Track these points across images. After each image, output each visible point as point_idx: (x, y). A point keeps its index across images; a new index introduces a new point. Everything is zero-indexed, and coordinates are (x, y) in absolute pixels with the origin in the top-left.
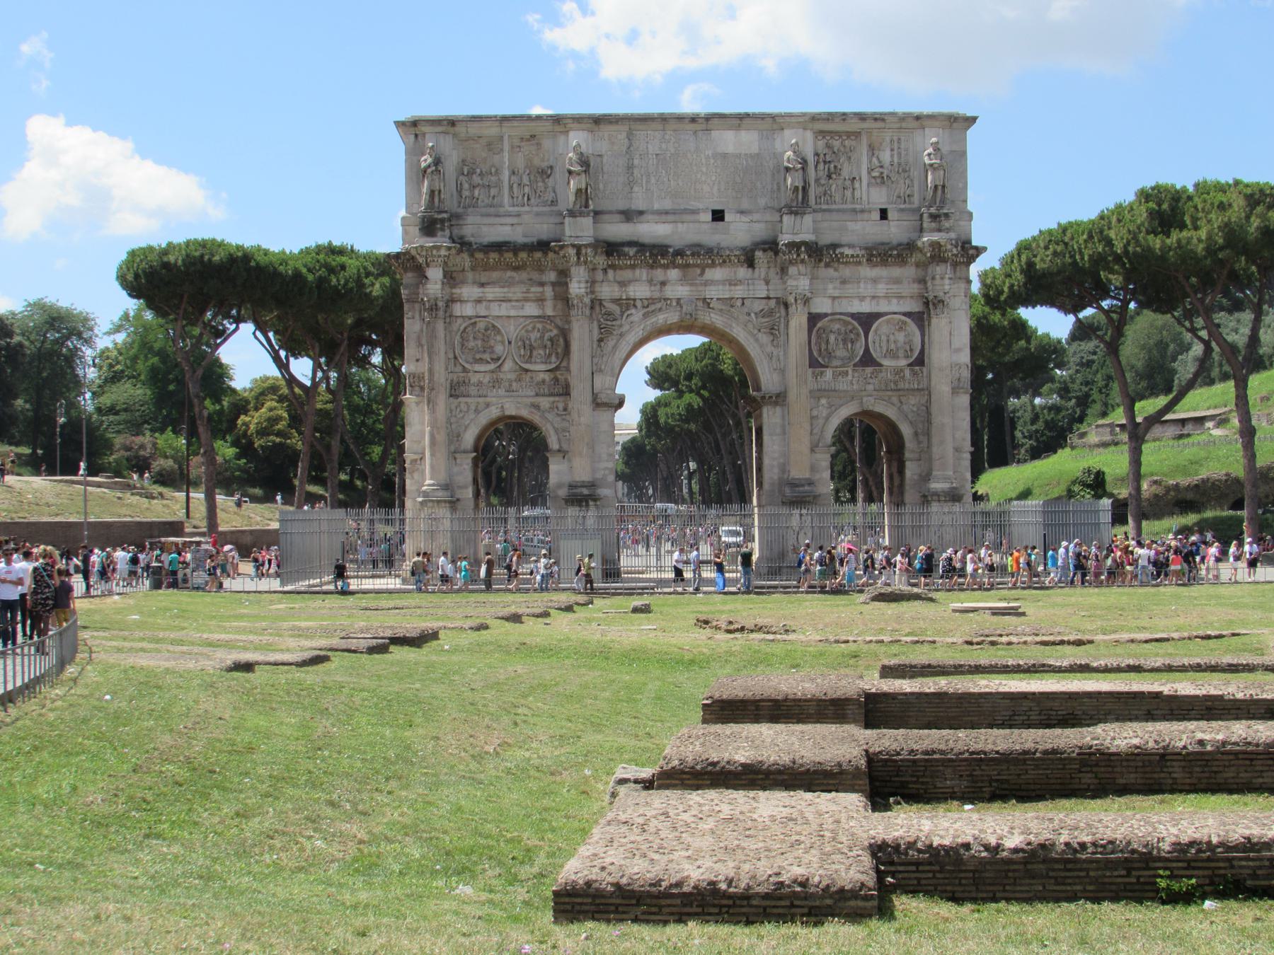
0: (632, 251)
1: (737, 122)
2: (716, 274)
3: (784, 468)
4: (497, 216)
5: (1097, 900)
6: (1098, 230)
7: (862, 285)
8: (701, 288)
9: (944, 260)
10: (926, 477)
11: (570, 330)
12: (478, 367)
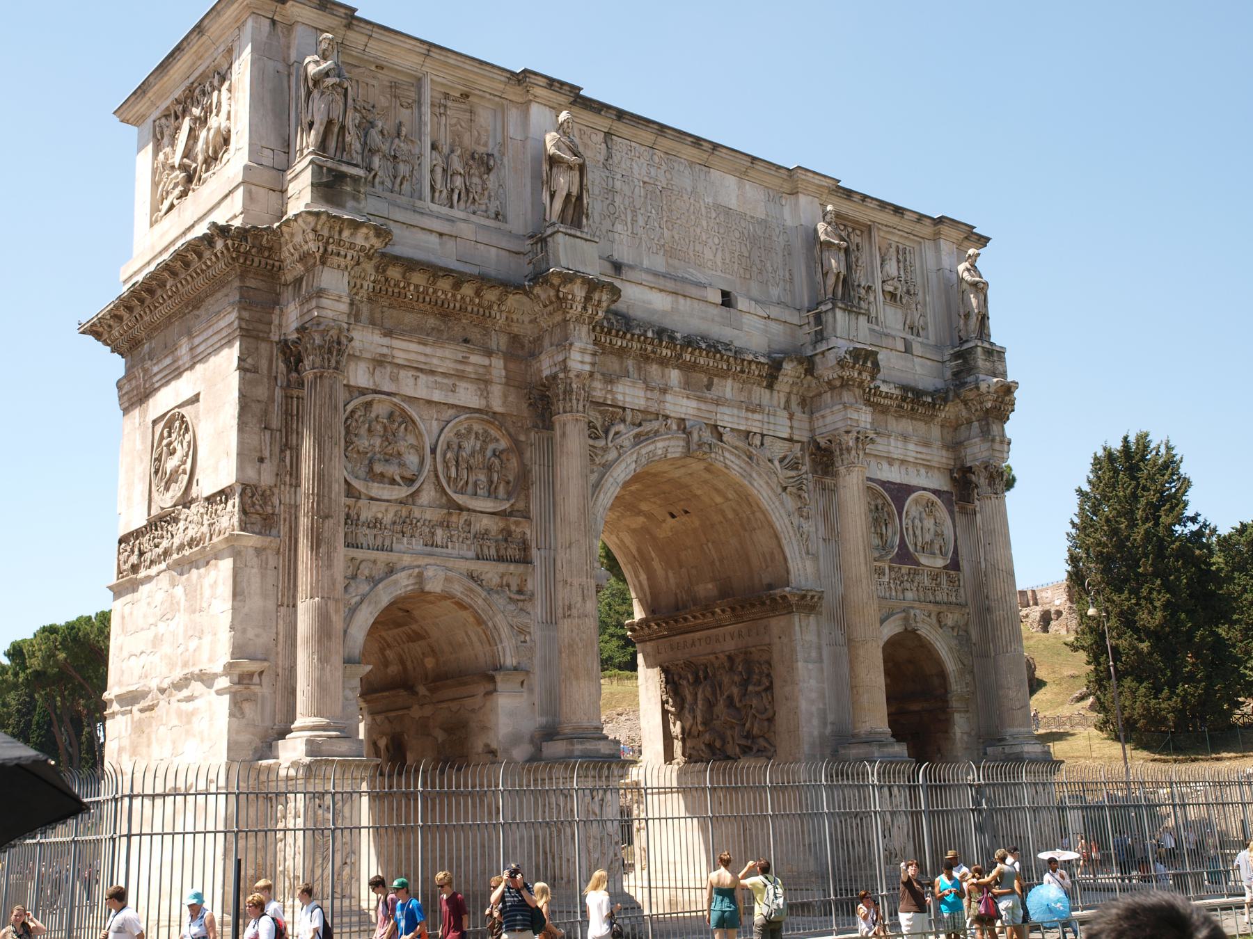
2: (727, 388)
4: (415, 210)
8: (712, 408)
12: (377, 490)
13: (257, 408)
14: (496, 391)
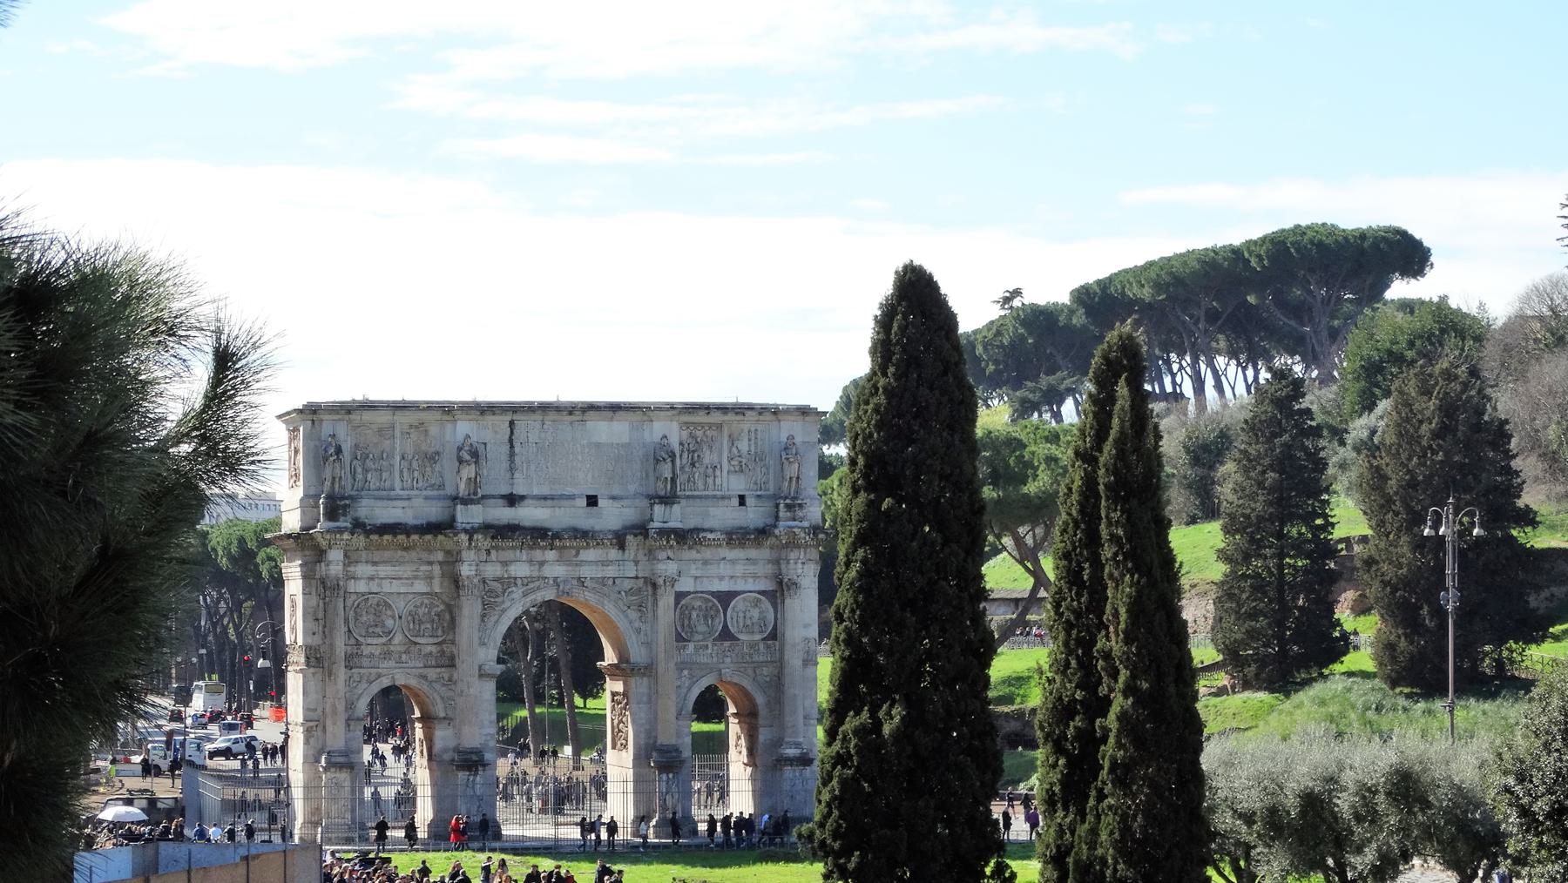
1: (610, 414)
2: (590, 554)
4: (390, 499)
7: (722, 566)
8: (577, 568)
9: (798, 547)
10: (778, 743)
11: (460, 607)
12: (370, 640)
13: (311, 610)
14: (436, 582)
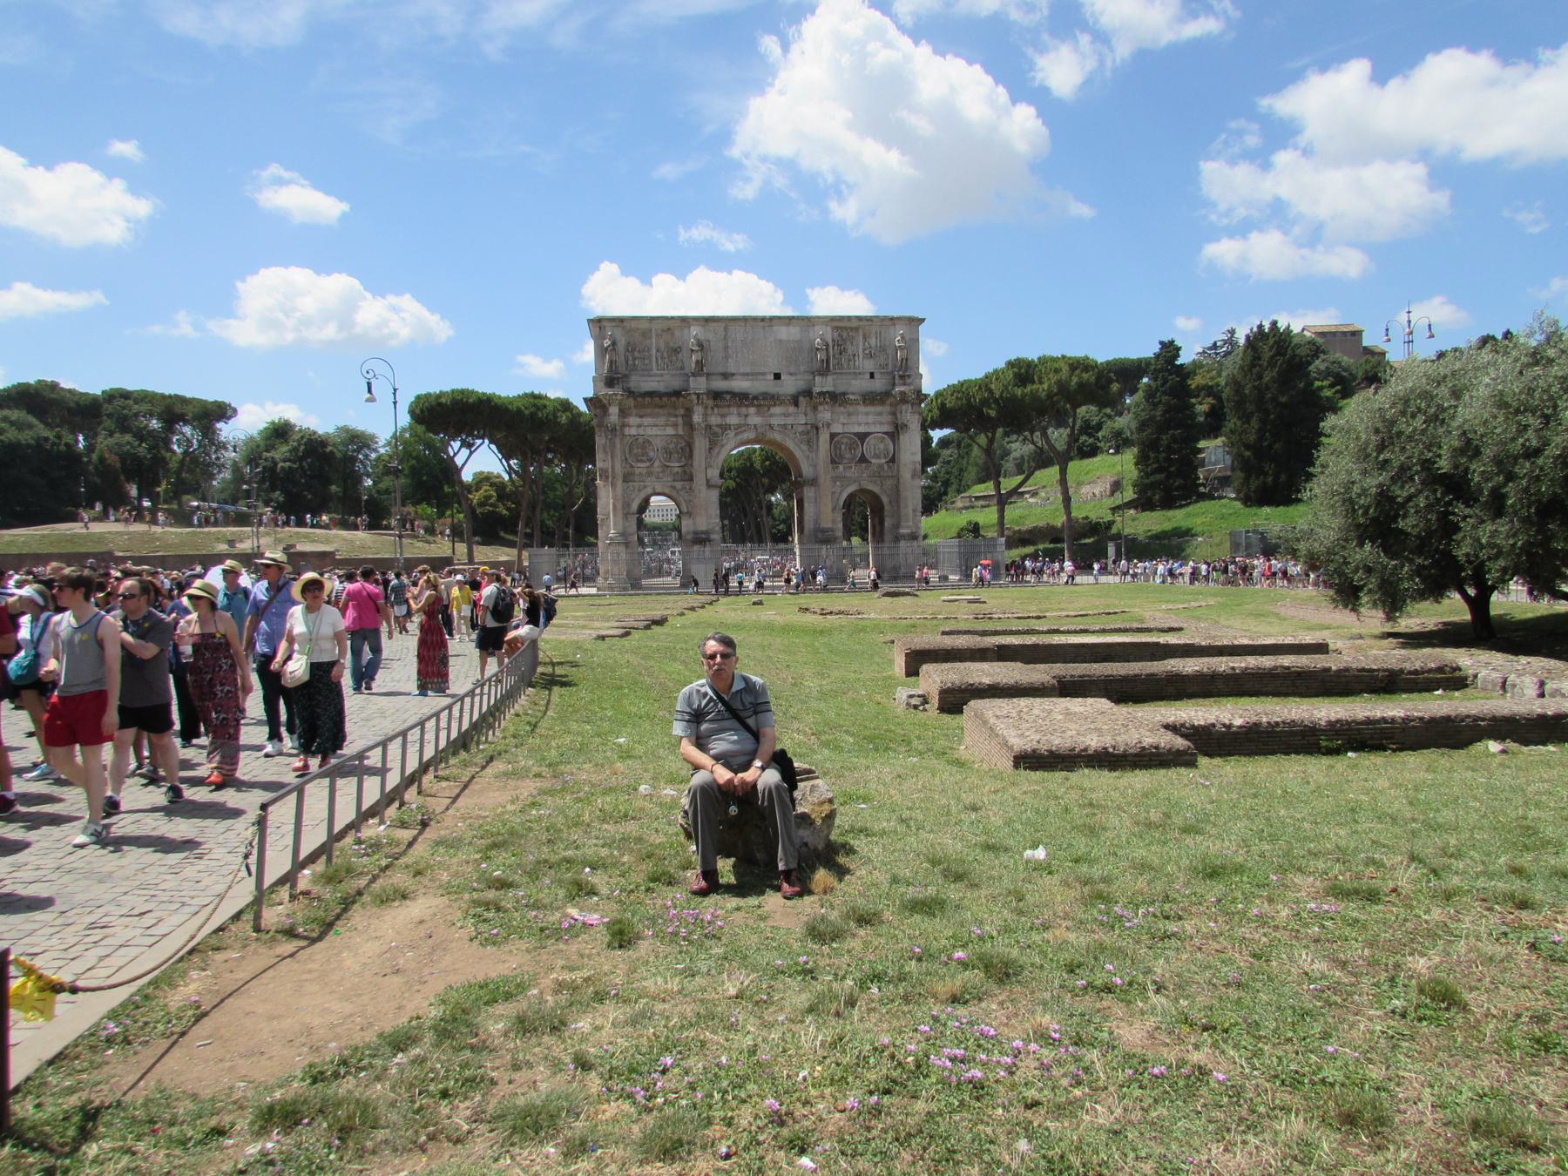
0: (728, 397)
2: (777, 410)
3: (817, 522)
5: (1287, 753)
6: (984, 384)
9: (907, 402)
10: (897, 526)
12: (640, 465)
